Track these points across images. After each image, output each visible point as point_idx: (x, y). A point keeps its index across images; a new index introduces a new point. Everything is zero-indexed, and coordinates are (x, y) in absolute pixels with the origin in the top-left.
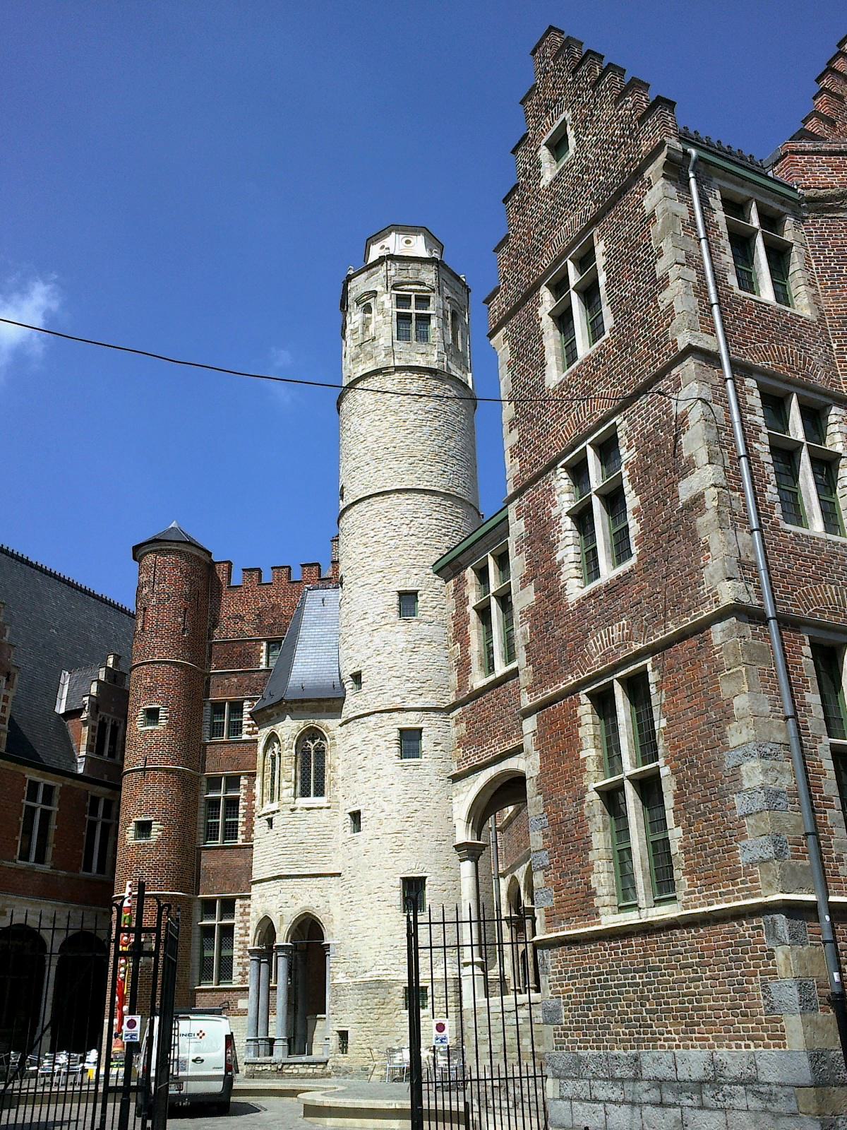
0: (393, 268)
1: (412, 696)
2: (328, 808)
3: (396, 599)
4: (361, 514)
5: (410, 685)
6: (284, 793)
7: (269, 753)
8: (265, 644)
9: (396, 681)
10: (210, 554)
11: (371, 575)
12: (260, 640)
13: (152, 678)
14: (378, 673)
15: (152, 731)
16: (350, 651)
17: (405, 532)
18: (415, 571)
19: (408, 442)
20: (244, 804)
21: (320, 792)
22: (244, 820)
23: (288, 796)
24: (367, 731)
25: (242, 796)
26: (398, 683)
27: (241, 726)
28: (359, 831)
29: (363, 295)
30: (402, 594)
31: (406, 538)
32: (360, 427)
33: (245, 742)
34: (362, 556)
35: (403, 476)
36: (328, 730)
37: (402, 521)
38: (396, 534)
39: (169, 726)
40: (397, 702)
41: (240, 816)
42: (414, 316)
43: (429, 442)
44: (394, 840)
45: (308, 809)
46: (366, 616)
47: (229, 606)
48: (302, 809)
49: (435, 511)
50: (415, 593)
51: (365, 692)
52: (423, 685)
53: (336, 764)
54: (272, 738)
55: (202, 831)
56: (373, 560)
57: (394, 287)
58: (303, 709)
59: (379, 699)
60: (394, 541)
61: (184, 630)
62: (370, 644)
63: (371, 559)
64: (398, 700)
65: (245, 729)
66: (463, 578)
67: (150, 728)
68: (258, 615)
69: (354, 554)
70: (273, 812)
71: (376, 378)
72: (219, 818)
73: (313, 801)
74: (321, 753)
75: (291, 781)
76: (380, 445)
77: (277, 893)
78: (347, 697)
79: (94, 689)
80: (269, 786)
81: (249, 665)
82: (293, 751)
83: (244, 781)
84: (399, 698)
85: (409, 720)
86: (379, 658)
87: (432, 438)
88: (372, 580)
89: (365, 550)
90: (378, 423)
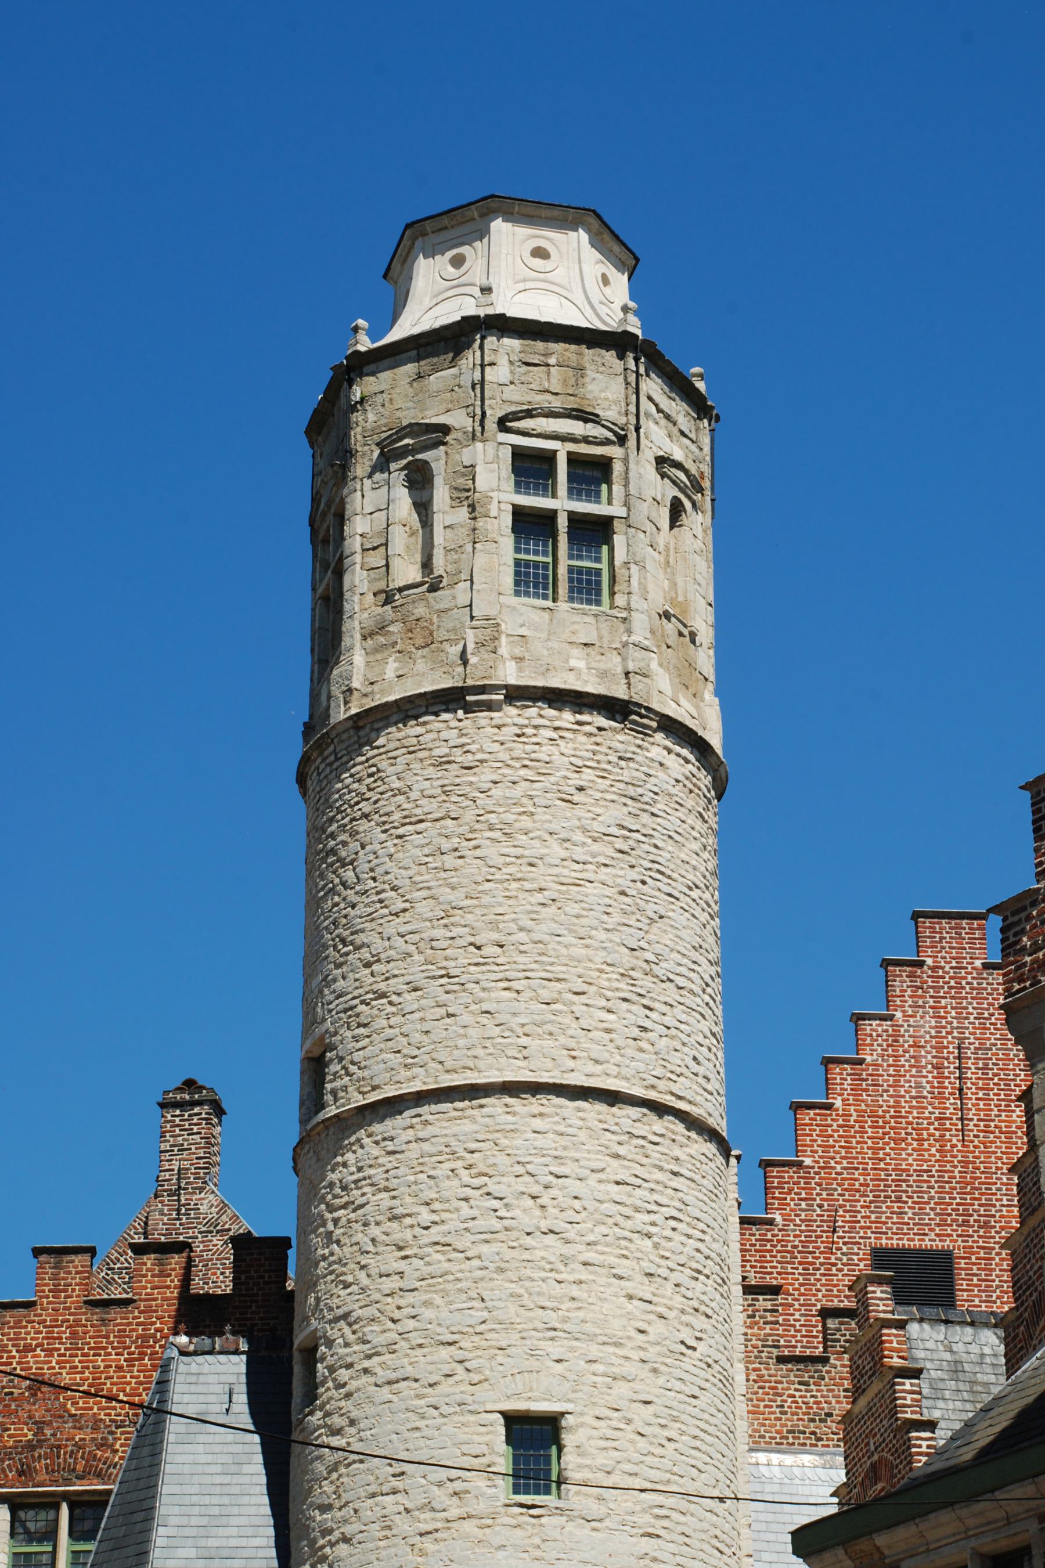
0: (503, 361)
4: (390, 1146)
11: (419, 1352)
17: (527, 1222)
18: (556, 1350)
29: (404, 431)
31: (528, 1241)
32: (389, 865)
35: (524, 1041)
38: (498, 1225)
42: (562, 522)
43: (602, 935)
49: (617, 1156)
56: (427, 1304)
57: (503, 424)
60: (494, 1247)
69: (362, 1275)
71: (445, 716)
76: (456, 931)
87: (611, 922)
89: (402, 1265)
90: (450, 861)
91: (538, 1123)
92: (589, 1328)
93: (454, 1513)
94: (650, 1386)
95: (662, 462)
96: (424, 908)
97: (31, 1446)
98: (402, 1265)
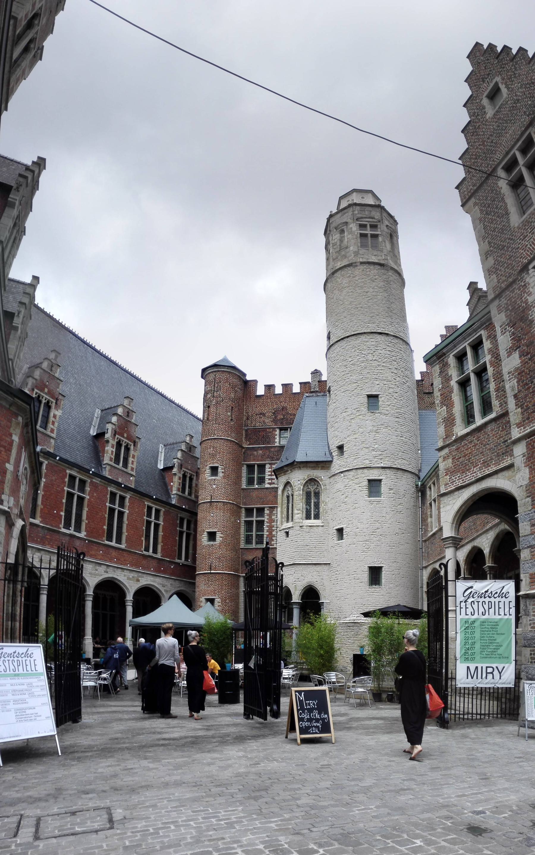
1: (376, 460)
2: (322, 526)
3: (366, 399)
4: (343, 347)
5: (375, 453)
6: (296, 517)
7: (286, 494)
8: (278, 431)
9: (367, 450)
10: (245, 375)
12: (275, 428)
13: (213, 448)
14: (355, 445)
15: (215, 480)
16: (336, 432)
17: (370, 358)
18: (377, 383)
19: (369, 304)
20: (267, 524)
21: (317, 517)
22: (268, 533)
23: (298, 519)
24: (348, 480)
25: (266, 520)
26: (367, 451)
27: (264, 479)
28: (342, 539)
30: (369, 396)
33: (267, 488)
34: (343, 374)
36: (322, 480)
37: (369, 352)
39: (224, 477)
40: (367, 463)
41: (265, 531)
44: (364, 545)
45: (310, 526)
46: (348, 410)
47: (256, 407)
48: (307, 526)
49: (388, 346)
50: (376, 396)
51: (346, 457)
52: (383, 453)
53: (327, 501)
54: (288, 484)
55: (243, 539)
58: (307, 467)
59: (355, 461)
61: (231, 420)
62: (349, 428)
63: (350, 375)
64: (367, 462)
65: (267, 481)
66: (447, 363)
67: (213, 478)
68: (274, 413)
70: (289, 528)
72: (252, 532)
73: (313, 522)
74: (317, 495)
75: (299, 510)
77: (292, 573)
78: (334, 460)
79: (179, 455)
80: (285, 513)
81: (268, 443)
82: (301, 492)
83: (267, 511)
84: (367, 461)
85: (374, 475)
86: (355, 436)
88: (350, 387)
89: (345, 369)
90: (351, 294)
91: (372, 340)
92: (384, 378)
93: (358, 414)
94: (398, 390)
95: (387, 226)
96: (346, 303)
97: (282, 419)
98: (345, 369)
